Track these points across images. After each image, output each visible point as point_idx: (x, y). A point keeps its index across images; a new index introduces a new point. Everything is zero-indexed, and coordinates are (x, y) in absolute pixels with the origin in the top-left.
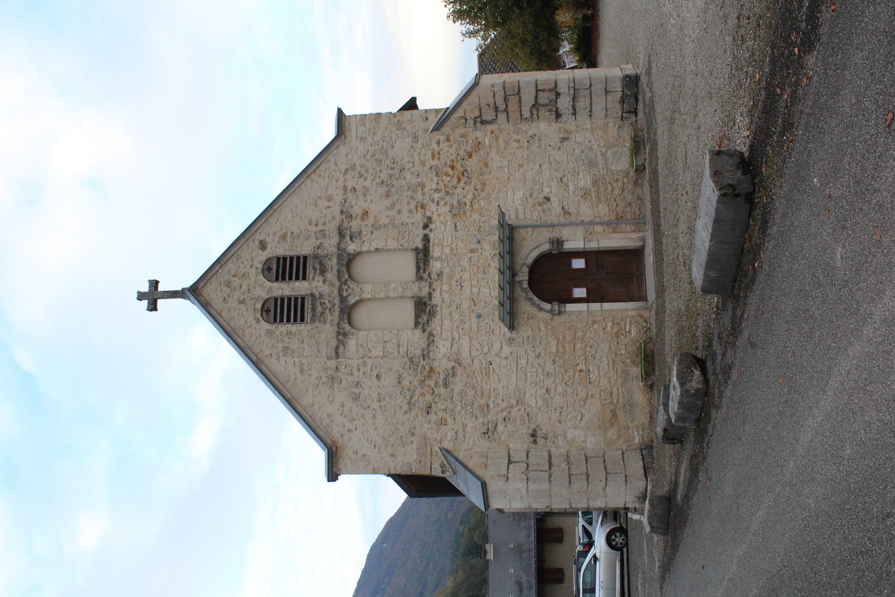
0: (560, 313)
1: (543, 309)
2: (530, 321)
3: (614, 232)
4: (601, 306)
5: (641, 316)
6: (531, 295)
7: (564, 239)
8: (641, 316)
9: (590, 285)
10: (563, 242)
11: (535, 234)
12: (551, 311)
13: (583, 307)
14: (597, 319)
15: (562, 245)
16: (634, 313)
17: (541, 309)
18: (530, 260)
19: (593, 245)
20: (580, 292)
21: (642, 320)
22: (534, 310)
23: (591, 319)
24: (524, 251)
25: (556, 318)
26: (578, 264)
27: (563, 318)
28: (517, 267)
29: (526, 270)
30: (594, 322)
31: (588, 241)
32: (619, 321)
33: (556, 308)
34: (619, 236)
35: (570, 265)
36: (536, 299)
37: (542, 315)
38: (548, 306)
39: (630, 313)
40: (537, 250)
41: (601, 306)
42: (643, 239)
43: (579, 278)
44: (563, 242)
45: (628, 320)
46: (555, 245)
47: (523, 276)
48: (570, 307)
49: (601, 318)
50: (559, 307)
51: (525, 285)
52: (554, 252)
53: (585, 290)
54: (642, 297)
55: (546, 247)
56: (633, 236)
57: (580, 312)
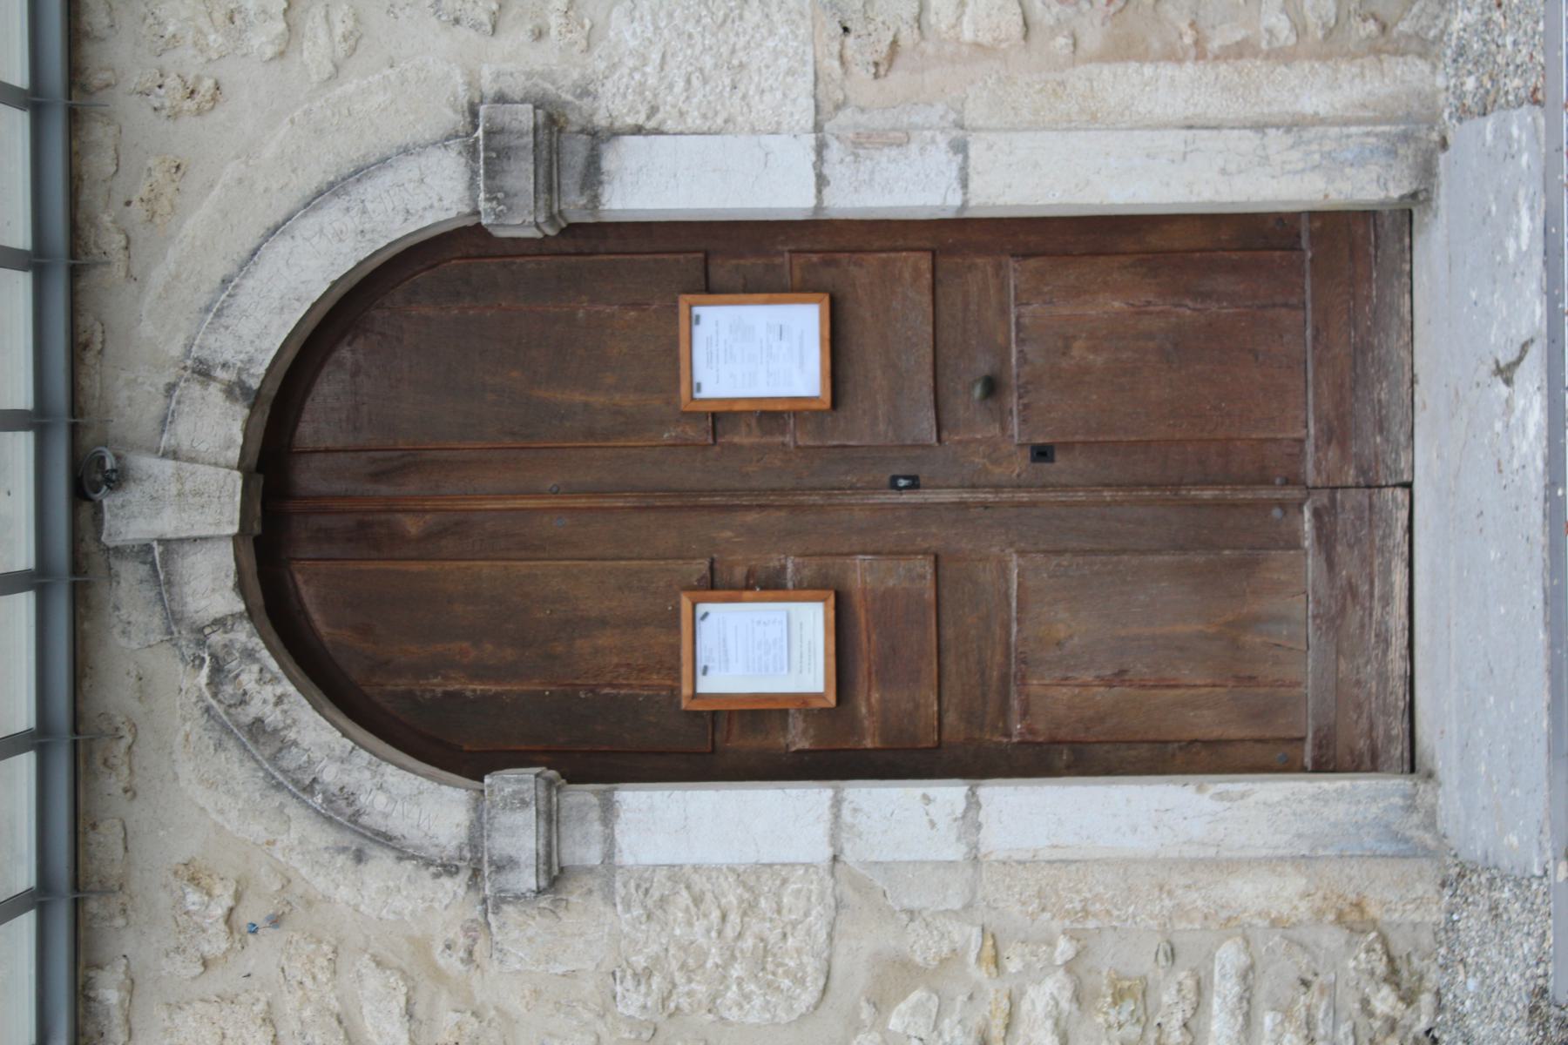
0: (555, 877)
1: (385, 839)
2: (263, 955)
3: (1123, 49)
4: (970, 819)
5: (1353, 919)
6: (269, 689)
7: (613, 106)
8: (1353, 919)
9: (862, 574)
10: (599, 138)
11: (317, 49)
12: (474, 864)
13: (774, 821)
14: (922, 947)
15: (592, 176)
16: (1287, 893)
17: (367, 840)
18: (260, 331)
19: (909, 184)
20: (759, 648)
21: (1360, 960)
22: (298, 844)
23: (863, 944)
24: (195, 224)
25: (523, 935)
26: (758, 352)
27: (588, 933)
28: (131, 394)
29: (219, 428)
30: (893, 977)
31: (862, 142)
32: (1142, 961)
33: (519, 835)
34: (1171, 88)
35: (671, 653)
36: (316, 734)
37: (380, 895)
38: (430, 806)
39: (1248, 893)
40: (332, 216)
41: (970, 819)
42: (1421, 143)
43: (752, 497)
44: (599, 138)
45: (1229, 956)
46: (521, 176)
47: (187, 497)
48: (663, 823)
49: (968, 936)
50: (550, 819)
51: (212, 586)
52: (521, 221)
53: (809, 622)
54: (1361, 735)
55: (434, 194)
56: (1316, 92)
57: (756, 879)
